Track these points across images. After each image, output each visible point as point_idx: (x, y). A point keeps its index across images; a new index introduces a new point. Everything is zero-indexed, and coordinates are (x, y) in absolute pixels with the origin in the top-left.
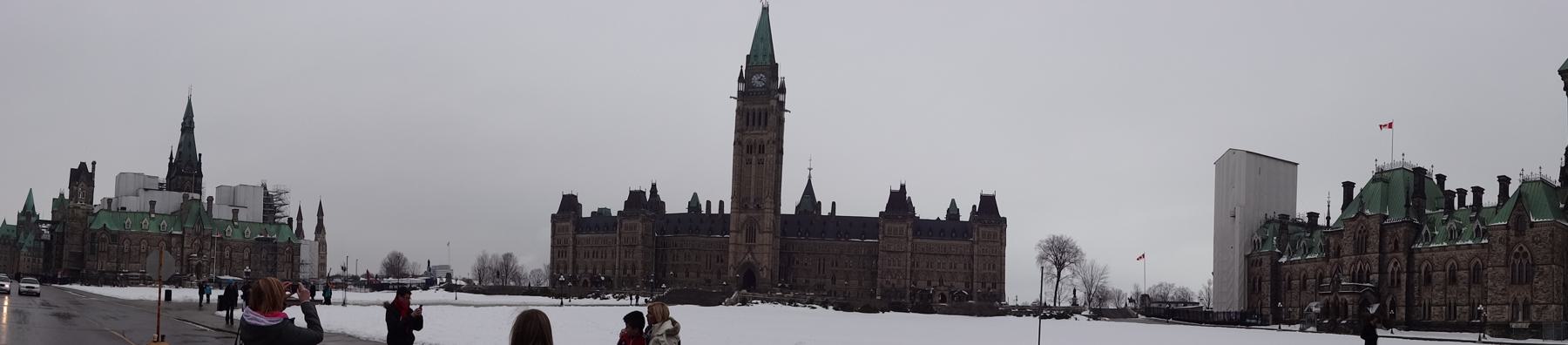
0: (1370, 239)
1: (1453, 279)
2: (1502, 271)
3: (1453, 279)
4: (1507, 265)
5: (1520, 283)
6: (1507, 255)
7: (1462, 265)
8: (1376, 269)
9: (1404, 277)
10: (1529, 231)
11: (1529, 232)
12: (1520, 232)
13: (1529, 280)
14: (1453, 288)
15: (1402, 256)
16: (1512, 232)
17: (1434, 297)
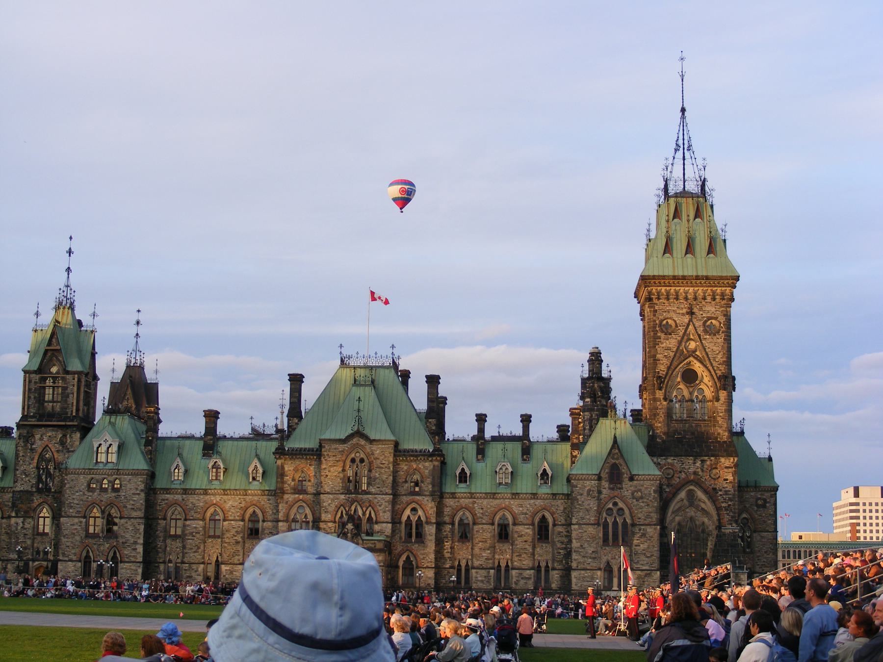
2: (591, 530)
7: (521, 518)
8: (387, 516)
9: (430, 531)
10: (626, 484)
11: (628, 487)
13: (627, 543)
14: (507, 547)
16: (605, 484)
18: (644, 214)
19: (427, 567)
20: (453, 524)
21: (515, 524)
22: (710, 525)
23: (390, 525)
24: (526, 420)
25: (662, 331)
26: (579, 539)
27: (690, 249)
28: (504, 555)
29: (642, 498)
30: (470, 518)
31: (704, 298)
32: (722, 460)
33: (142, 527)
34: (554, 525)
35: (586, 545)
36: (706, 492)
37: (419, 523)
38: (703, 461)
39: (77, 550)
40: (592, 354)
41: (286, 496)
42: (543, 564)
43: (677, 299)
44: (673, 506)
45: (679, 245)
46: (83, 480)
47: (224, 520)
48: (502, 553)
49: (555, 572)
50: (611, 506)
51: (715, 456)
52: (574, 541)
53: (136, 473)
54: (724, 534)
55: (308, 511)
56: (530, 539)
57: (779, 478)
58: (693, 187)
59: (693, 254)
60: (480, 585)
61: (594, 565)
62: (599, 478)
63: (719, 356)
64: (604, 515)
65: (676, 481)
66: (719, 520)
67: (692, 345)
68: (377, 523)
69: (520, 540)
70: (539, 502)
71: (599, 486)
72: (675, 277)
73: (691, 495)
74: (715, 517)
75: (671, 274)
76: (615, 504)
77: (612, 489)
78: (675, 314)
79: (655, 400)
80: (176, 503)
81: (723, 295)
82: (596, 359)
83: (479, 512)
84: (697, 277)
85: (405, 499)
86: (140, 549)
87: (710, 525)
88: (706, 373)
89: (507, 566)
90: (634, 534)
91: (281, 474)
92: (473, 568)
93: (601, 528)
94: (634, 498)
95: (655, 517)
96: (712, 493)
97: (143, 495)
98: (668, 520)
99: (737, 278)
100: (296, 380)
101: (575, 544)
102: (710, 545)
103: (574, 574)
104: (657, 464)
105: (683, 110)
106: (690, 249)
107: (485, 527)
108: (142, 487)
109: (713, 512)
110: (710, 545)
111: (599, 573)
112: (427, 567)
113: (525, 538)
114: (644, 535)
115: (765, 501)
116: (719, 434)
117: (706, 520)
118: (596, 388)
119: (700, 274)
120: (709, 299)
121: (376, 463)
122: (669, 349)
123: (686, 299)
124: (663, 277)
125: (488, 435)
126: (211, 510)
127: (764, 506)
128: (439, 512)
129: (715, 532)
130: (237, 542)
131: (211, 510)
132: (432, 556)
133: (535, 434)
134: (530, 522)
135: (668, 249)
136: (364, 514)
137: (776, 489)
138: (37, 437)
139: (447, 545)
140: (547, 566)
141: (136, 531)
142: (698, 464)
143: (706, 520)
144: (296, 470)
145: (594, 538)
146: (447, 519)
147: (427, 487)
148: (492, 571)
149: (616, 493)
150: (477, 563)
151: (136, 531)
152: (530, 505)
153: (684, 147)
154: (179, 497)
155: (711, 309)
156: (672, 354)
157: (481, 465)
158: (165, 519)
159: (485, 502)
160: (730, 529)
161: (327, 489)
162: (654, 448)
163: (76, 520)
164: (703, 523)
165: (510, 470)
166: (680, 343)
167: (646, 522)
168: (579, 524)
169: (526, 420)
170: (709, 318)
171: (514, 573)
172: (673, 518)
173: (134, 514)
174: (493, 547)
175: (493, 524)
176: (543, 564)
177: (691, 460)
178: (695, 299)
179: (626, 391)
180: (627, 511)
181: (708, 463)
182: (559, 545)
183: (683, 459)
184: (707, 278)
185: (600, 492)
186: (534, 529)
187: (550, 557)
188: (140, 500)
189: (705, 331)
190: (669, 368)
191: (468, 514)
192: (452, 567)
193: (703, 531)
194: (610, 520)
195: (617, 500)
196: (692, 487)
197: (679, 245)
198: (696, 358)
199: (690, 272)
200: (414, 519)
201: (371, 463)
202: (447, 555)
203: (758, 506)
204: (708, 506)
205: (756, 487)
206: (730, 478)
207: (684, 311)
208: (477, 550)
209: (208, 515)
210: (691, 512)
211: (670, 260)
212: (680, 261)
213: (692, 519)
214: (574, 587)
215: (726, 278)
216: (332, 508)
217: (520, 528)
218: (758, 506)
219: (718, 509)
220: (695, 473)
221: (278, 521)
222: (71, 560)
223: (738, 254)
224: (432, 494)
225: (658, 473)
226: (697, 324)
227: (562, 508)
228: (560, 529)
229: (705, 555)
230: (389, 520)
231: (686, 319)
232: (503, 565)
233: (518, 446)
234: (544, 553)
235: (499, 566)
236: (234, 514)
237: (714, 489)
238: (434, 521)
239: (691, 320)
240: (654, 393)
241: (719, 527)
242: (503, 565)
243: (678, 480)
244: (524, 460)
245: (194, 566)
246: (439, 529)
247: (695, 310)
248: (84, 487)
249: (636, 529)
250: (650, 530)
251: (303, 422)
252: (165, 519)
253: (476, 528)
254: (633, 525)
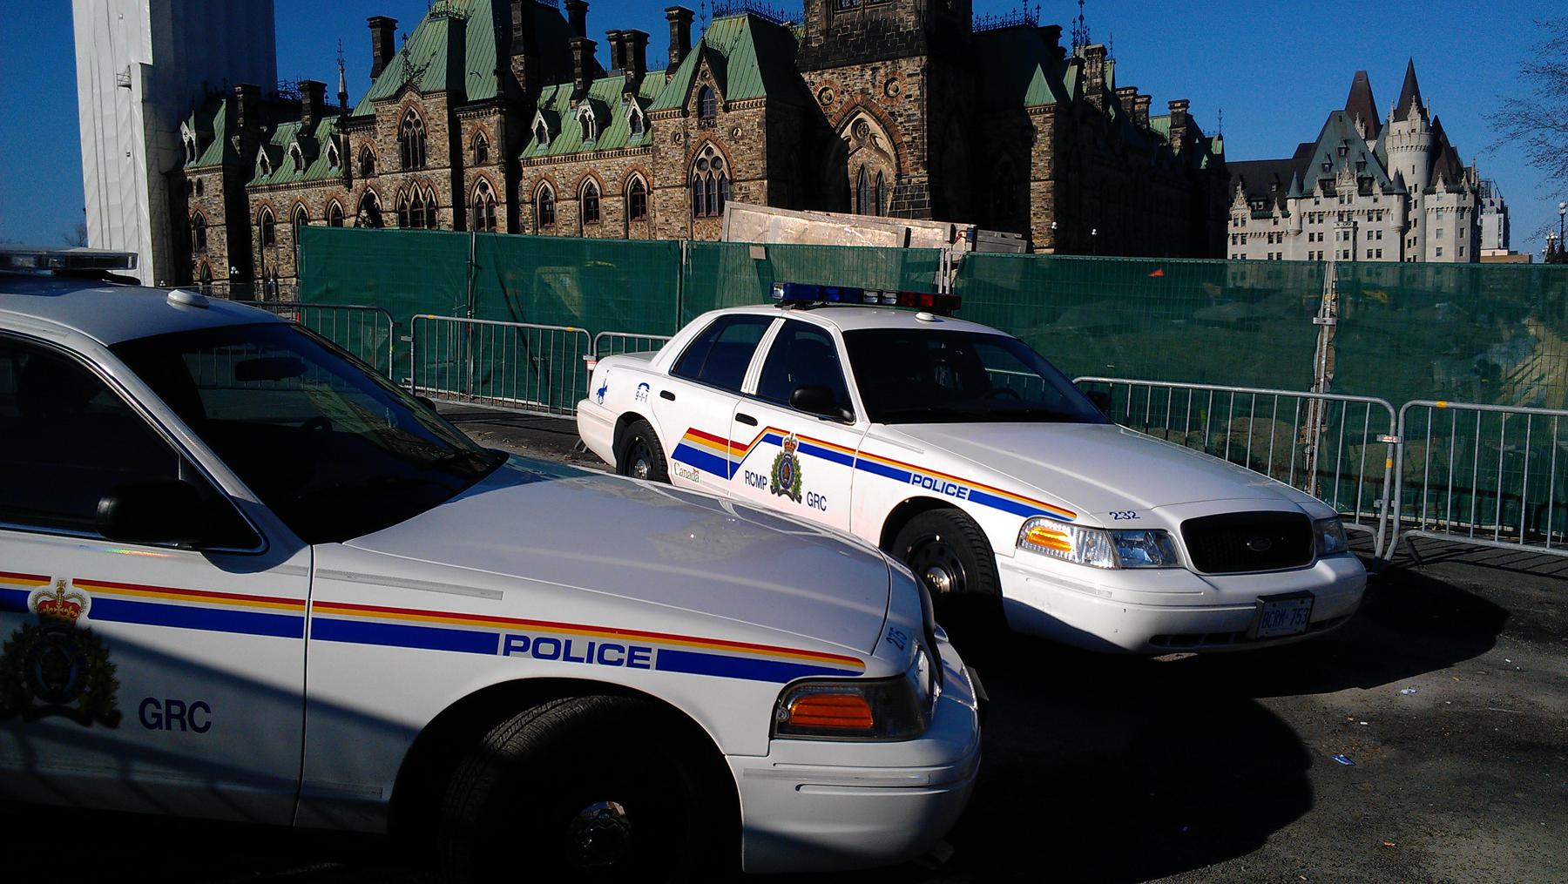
16: (693, 121)
26: (664, 209)
32: (903, 63)
38: (874, 70)
51: (893, 58)
70: (629, 160)
83: (560, 182)
107: (570, 203)
113: (615, 216)
116: (901, 20)
121: (431, 125)
146: (526, 197)
159: (566, 166)
181: (882, 71)
188: (220, 201)
206: (915, 92)
216: (391, 194)
237: (892, 114)
243: (839, 106)
249: (736, 186)
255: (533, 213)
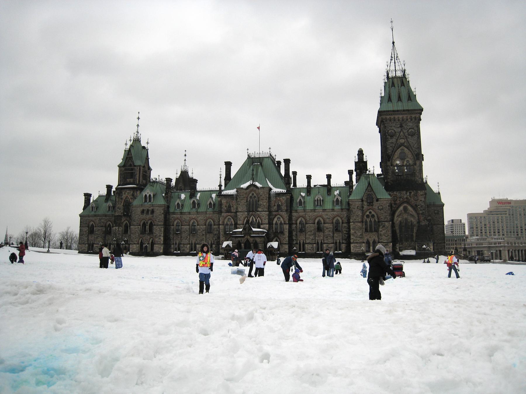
0: (261, 202)
1: (319, 229)
2: (359, 224)
3: (319, 229)
4: (362, 222)
5: (371, 231)
6: (363, 216)
7: (327, 221)
8: (267, 221)
9: (286, 227)
10: (375, 203)
11: (376, 205)
12: (370, 204)
13: (377, 231)
14: (321, 234)
15: (285, 215)
16: (365, 203)
17: (487, 254)
18: (379, 88)
19: (285, 244)
20: (296, 224)
21: (324, 223)
22: (414, 221)
23: (268, 225)
24: (329, 177)
25: (389, 135)
26: (354, 229)
27: (400, 99)
28: (320, 237)
29: (382, 209)
30: (304, 221)
31: (407, 120)
32: (419, 192)
33: (163, 229)
34: (343, 223)
35: (357, 232)
36: (412, 206)
37: (281, 224)
38: (410, 193)
39: (137, 239)
40: (359, 151)
41: (223, 214)
42: (338, 241)
43: (395, 120)
44: (397, 214)
45: (394, 98)
46: (139, 210)
47: (198, 225)
48: (319, 236)
49: (343, 245)
50: (368, 213)
52: (352, 230)
53: (160, 206)
54: (421, 225)
55: (232, 220)
56: (331, 230)
57: (443, 200)
58: (399, 74)
59: (401, 101)
60: (309, 251)
61: (361, 241)
62: (362, 201)
63: (416, 145)
64: (365, 217)
65: (398, 202)
66: (419, 219)
67: (402, 141)
68: (262, 224)
69: (327, 230)
70: (335, 213)
71: (363, 204)
72: (394, 111)
73: (405, 209)
74: (417, 218)
75: (392, 109)
76: (370, 213)
77: (368, 206)
78: (394, 128)
79: (387, 166)
80: (178, 219)
81: (415, 118)
82: (361, 153)
83: (308, 218)
84: (404, 111)
85: (274, 213)
86: (162, 238)
87: (414, 221)
88: (410, 153)
89: (321, 242)
90: (379, 226)
91: (220, 204)
92: (306, 244)
93: (364, 223)
94: (379, 209)
95: (389, 218)
96: (415, 208)
97: (163, 215)
98: (395, 220)
99: (422, 110)
100: (228, 165)
101: (352, 231)
102: (415, 231)
103: (352, 245)
104: (390, 195)
105: (393, 43)
106: (400, 99)
108: (162, 212)
109: (416, 215)
110: (415, 231)
111: (364, 244)
112: (285, 244)
113: (329, 230)
114: (384, 226)
115: (438, 211)
117: (412, 219)
118: (361, 165)
119: (405, 109)
120: (409, 120)
122: (392, 143)
123: (399, 120)
124: (388, 111)
125: (312, 186)
126: (192, 221)
127: (438, 213)
128: (290, 219)
129: (417, 225)
130: (203, 235)
131: (192, 221)
132: (287, 239)
133: (333, 183)
134: (331, 222)
135: (390, 100)
136: (256, 220)
137: (443, 205)
138: (123, 193)
139: (294, 233)
140: (340, 242)
141: (160, 230)
142: (408, 194)
143: (412, 219)
144: (227, 203)
145: (361, 228)
146: (294, 222)
147: (284, 208)
148: (314, 245)
149: (371, 207)
150: (308, 241)
151: (160, 230)
152: (331, 214)
153: (394, 58)
154: (179, 216)
155: (410, 124)
156: (394, 145)
157: (309, 197)
158: (173, 225)
159: (311, 214)
160: (423, 223)
161: (240, 210)
162: (388, 188)
163: (137, 227)
164: (411, 221)
165: (322, 199)
166: (397, 140)
167: (385, 220)
168: (354, 222)
169: (329, 177)
170: (410, 129)
171: (325, 245)
172: (397, 220)
173: (160, 224)
174: (315, 234)
175: (314, 223)
176: (338, 241)
177: (404, 192)
178: (403, 120)
179: (374, 167)
180: (376, 216)
181: (413, 193)
182: (345, 232)
183: (402, 192)
184: (408, 110)
185: (363, 207)
186: (333, 225)
187: (341, 237)
188: (162, 217)
189: (409, 135)
190: (392, 151)
191: (303, 219)
192: (297, 243)
193: (412, 224)
194: (368, 220)
195: (371, 211)
196: (405, 205)
197: (394, 98)
198: (405, 146)
199: (400, 108)
200: (279, 222)
201: (258, 198)
202: (294, 238)
203: (435, 213)
204: (414, 213)
205: (434, 205)
207: (399, 126)
208: (307, 236)
209: (191, 223)
210: (405, 216)
211: (391, 104)
212: (396, 104)
213: (406, 219)
214: (352, 251)
215: (417, 110)
216: (242, 219)
217: (326, 225)
218: (435, 213)
219: (418, 214)
220: (407, 198)
221: (219, 225)
222: (135, 244)
223: (421, 100)
224: (287, 211)
225: (389, 197)
226: (405, 131)
227: (346, 215)
228: (345, 225)
229: (412, 235)
230: (267, 223)
231: (399, 130)
232: (320, 242)
233: (326, 189)
234: (338, 237)
235: (318, 242)
236: (202, 222)
237: (416, 205)
238: (287, 222)
239: (401, 130)
240: (386, 163)
241: (419, 222)
242: (320, 242)
244: (328, 195)
245: (185, 246)
246: (290, 227)
247: (403, 125)
248: (139, 213)
250: (386, 224)
251: (231, 181)
252: (173, 225)
253: (307, 225)
254: (379, 222)
255: (296, 227)
